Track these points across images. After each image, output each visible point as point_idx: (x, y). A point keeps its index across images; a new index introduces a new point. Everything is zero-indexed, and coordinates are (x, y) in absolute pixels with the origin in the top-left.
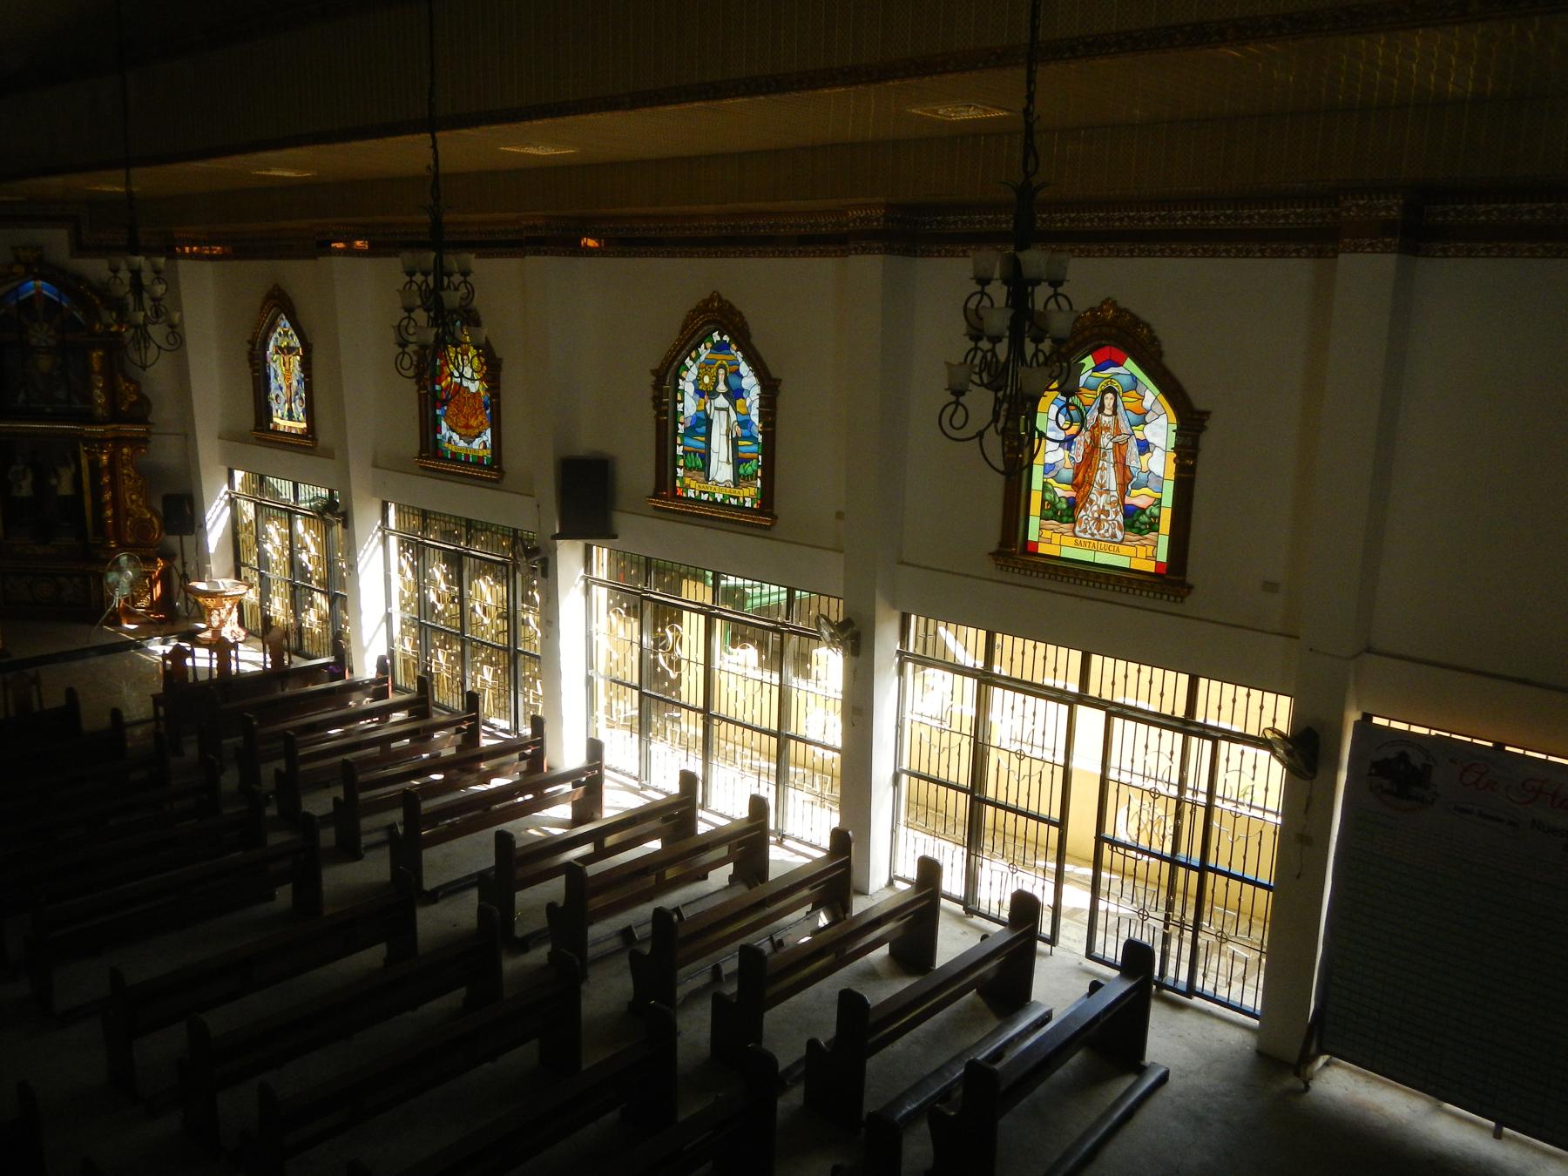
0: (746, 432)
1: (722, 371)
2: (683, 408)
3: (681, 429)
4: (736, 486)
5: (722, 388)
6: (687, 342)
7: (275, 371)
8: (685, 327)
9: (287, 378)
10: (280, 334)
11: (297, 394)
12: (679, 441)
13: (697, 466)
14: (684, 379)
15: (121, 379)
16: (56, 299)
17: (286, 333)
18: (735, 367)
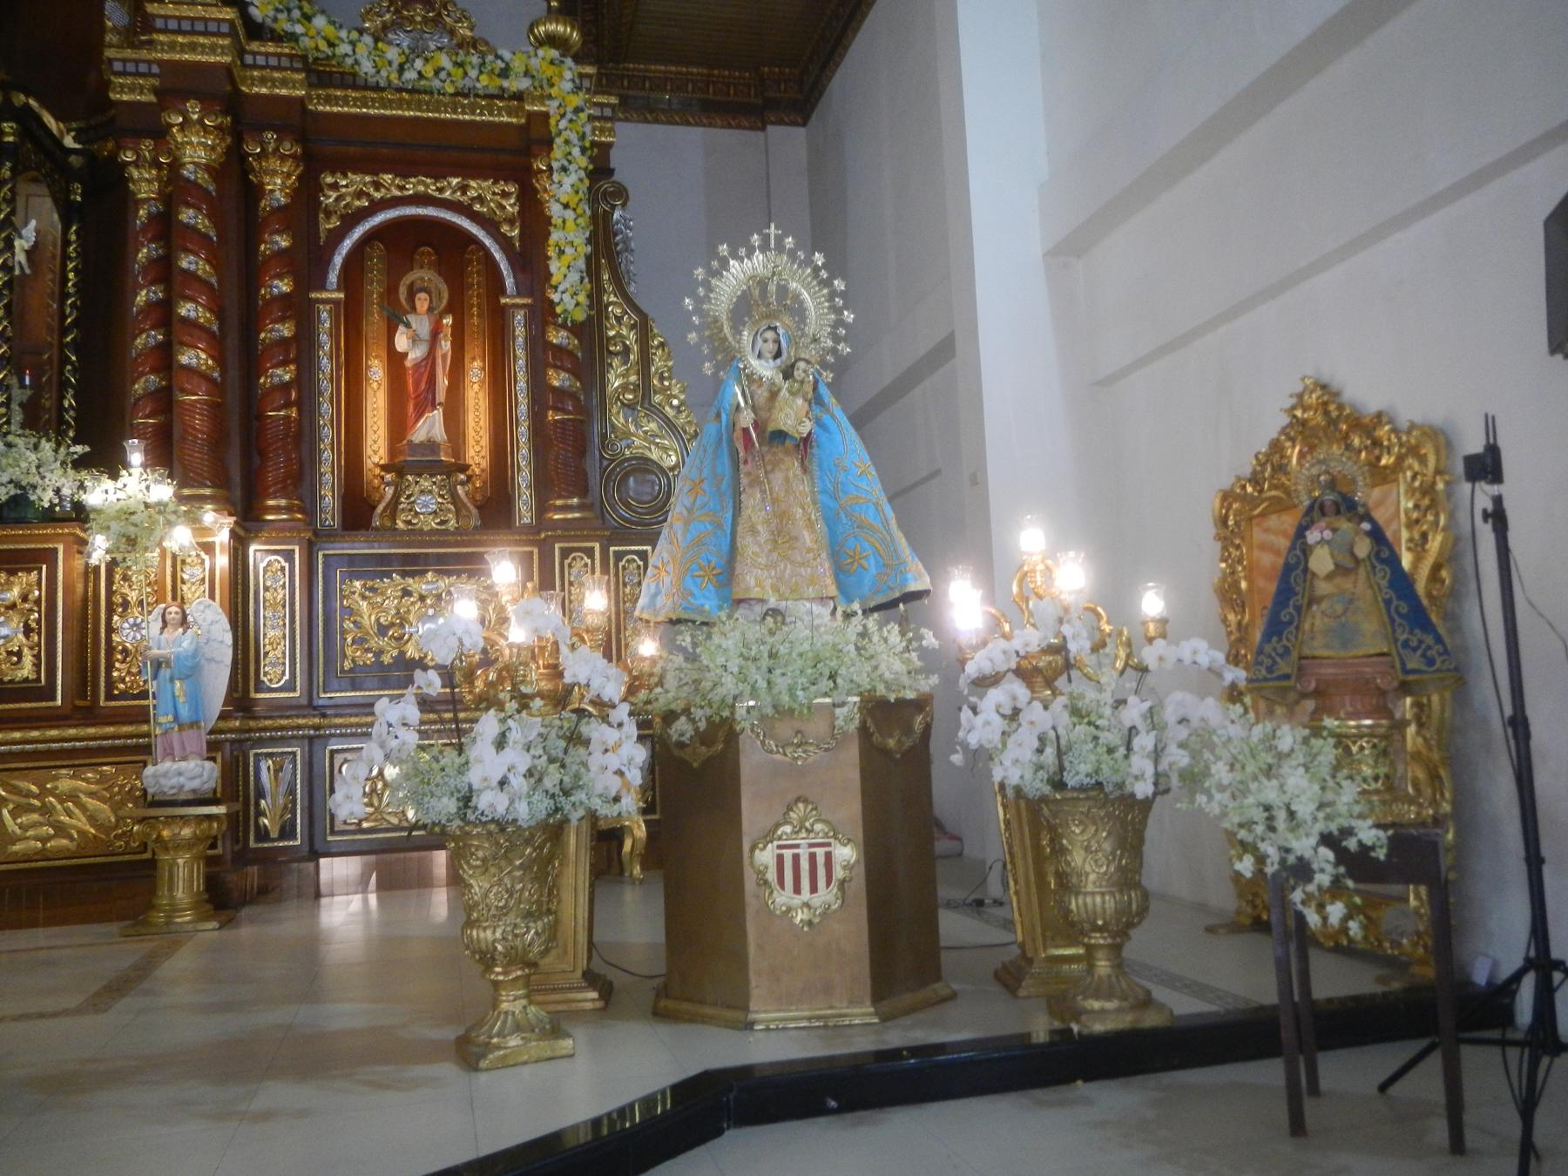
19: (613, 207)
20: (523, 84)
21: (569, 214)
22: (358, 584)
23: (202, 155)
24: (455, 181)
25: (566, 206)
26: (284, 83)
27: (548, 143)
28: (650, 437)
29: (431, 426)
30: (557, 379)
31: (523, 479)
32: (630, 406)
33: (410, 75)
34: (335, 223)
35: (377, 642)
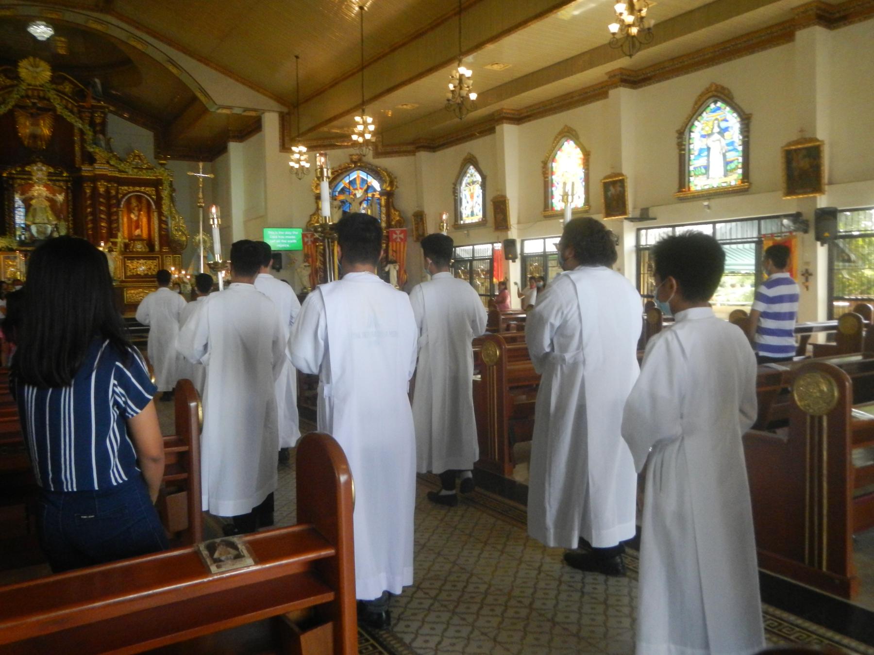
0: (731, 148)
1: (716, 122)
2: (694, 147)
3: (692, 157)
4: (725, 176)
5: (716, 130)
6: (695, 113)
7: (465, 195)
8: (696, 103)
9: (472, 196)
10: (469, 177)
11: (476, 202)
12: (691, 163)
13: (702, 173)
14: (693, 132)
15: (392, 211)
16: (365, 178)
17: (472, 175)
18: (723, 118)
19: (173, 193)
20: (158, 174)
21: (166, 198)
22: (129, 261)
23: (104, 190)
24: (143, 188)
25: (166, 196)
26: (115, 173)
27: (162, 184)
28: (180, 235)
29: (138, 232)
30: (164, 226)
31: (157, 243)
32: (176, 230)
33: (138, 174)
34: (121, 195)
35: (132, 271)
